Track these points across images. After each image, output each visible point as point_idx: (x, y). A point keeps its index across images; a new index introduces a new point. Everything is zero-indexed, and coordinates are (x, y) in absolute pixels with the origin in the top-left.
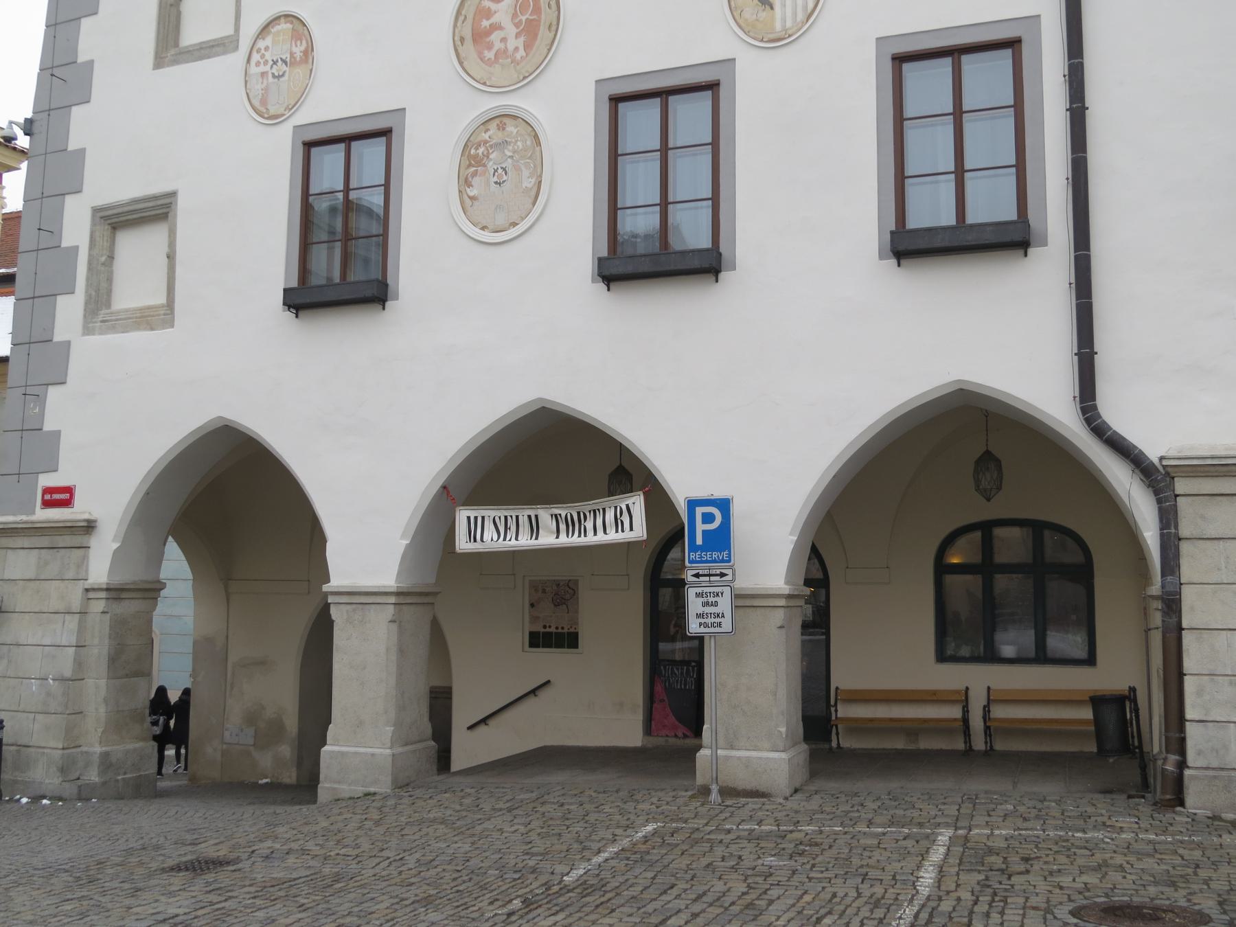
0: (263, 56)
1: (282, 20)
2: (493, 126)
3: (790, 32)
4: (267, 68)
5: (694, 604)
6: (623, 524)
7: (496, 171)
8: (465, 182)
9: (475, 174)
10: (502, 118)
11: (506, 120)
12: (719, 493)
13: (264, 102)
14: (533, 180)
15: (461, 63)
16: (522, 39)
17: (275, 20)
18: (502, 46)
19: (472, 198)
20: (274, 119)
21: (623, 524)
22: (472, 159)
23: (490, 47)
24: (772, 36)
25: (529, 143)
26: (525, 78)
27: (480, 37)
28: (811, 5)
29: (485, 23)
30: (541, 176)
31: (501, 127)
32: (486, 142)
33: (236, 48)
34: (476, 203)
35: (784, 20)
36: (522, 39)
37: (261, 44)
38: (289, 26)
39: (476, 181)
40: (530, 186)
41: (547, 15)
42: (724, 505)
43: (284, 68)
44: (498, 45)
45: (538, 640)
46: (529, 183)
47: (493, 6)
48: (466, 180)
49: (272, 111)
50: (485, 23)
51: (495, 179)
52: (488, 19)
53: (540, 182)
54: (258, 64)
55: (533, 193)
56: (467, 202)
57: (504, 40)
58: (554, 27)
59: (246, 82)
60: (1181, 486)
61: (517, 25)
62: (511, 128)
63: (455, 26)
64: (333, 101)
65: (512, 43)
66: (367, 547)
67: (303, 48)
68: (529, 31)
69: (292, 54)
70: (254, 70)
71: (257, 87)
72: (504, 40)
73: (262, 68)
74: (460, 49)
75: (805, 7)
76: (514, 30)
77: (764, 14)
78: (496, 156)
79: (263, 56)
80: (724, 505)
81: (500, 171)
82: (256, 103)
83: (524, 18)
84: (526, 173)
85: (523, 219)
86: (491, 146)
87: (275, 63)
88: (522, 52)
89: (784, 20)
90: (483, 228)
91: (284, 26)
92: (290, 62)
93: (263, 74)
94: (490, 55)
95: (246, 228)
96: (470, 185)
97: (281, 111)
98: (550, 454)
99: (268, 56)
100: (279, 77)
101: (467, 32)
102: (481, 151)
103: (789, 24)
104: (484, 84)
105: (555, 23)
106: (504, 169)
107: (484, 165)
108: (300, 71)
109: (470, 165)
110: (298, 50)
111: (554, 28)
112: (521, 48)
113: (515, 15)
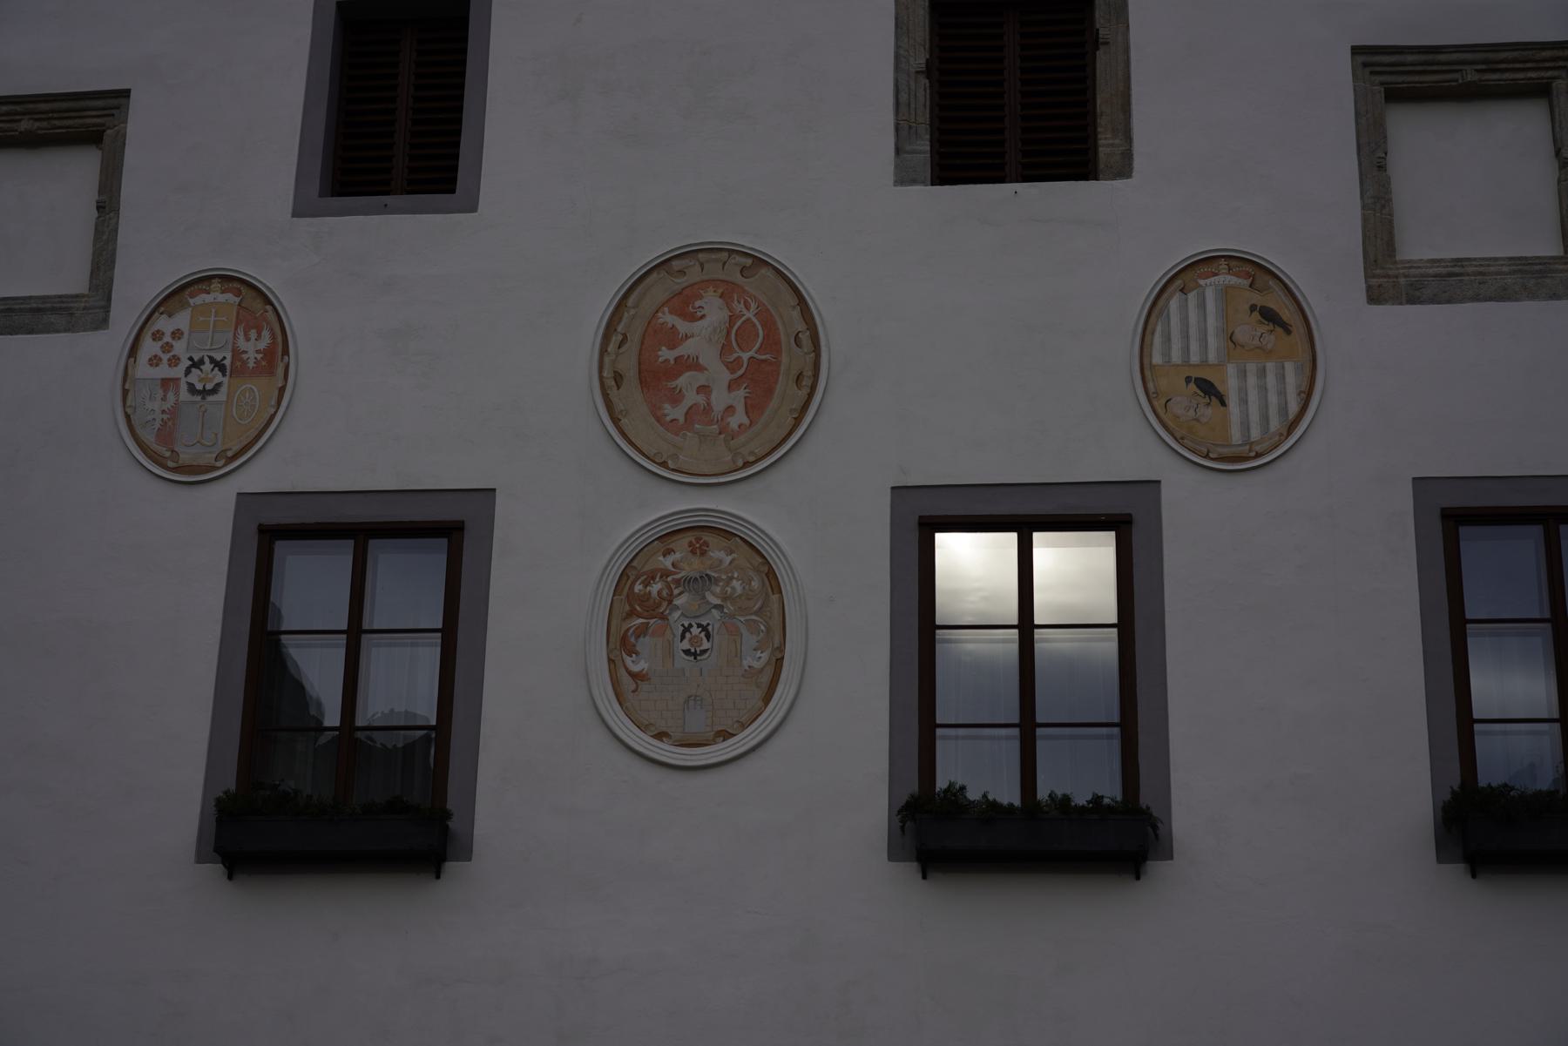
0: (167, 348)
1: (216, 285)
2: (682, 544)
3: (1258, 448)
4: (179, 372)
7: (687, 630)
8: (622, 644)
9: (642, 631)
11: (706, 537)
14: (765, 656)
15: (616, 421)
16: (741, 393)
18: (701, 399)
19: (635, 676)
20: (194, 474)
22: (637, 602)
23: (676, 398)
24: (1226, 451)
25: (755, 584)
26: (747, 464)
27: (655, 378)
28: (1293, 408)
29: (666, 354)
30: (781, 648)
31: (699, 550)
32: (665, 574)
33: (102, 323)
34: (644, 686)
35: (1246, 426)
36: (741, 393)
37: (164, 324)
38: (230, 297)
39: (644, 644)
40: (757, 665)
43: (218, 377)
44: (691, 398)
46: (757, 660)
47: (682, 326)
48: (624, 639)
49: (186, 457)
50: (666, 354)
51: (686, 645)
52: (672, 347)
53: (780, 661)
54: (154, 361)
55: (765, 679)
56: (627, 686)
57: (704, 389)
58: (809, 379)
59: (125, 393)
61: (732, 366)
62: (717, 554)
63: (603, 351)
65: (720, 399)
67: (264, 343)
68: (757, 382)
69: (237, 353)
70: (142, 369)
71: (152, 407)
72: (704, 389)
73: (164, 371)
74: (614, 393)
75: (1283, 410)
76: (726, 376)
77: (1209, 412)
79: (167, 348)
81: (695, 630)
82: (149, 438)
83: (745, 356)
84: (750, 640)
85: (744, 726)
86: (677, 582)
87: (196, 364)
88: (739, 418)
89: (1246, 426)
90: (660, 736)
91: (217, 296)
92: (236, 368)
93: (166, 383)
94: (676, 413)
96: (631, 651)
97: (209, 458)
99: (179, 348)
100: (204, 393)
101: (628, 364)
102: (655, 588)
103: (1255, 434)
104: (664, 464)
105: (808, 373)
106: (704, 628)
107: (663, 617)
109: (632, 614)
110: (252, 348)
111: (807, 382)
112: (740, 409)
113: (725, 349)
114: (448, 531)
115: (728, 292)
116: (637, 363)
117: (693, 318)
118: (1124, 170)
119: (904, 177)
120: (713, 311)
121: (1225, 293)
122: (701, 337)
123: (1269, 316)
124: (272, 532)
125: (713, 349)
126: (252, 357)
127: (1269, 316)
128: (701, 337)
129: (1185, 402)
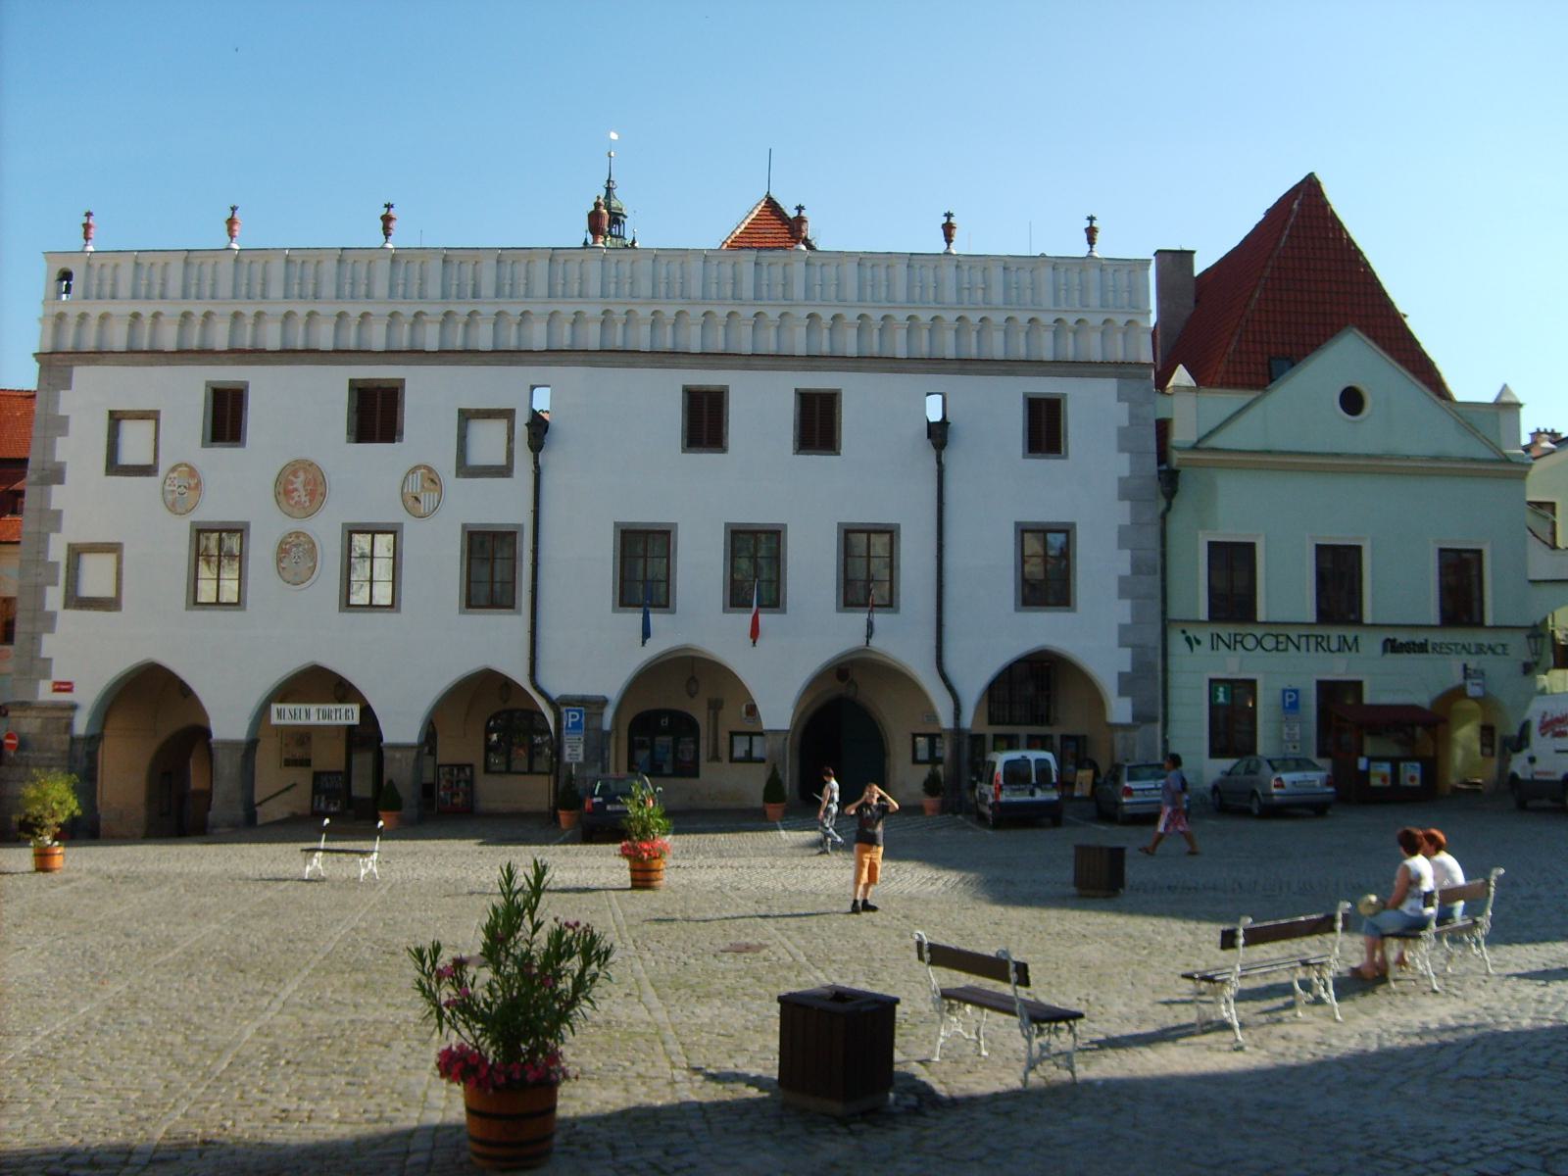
8: (279, 560)
10: (298, 534)
13: (173, 505)
17: (180, 465)
21: (348, 715)
22: (283, 551)
27: (288, 493)
29: (291, 487)
31: (298, 537)
39: (286, 560)
41: (320, 489)
44: (297, 499)
45: (289, 763)
46: (311, 564)
49: (179, 510)
56: (281, 571)
58: (324, 495)
60: (563, 709)
64: (213, 510)
65: (303, 499)
66: (228, 724)
68: (312, 494)
71: (170, 497)
73: (171, 488)
77: (417, 505)
88: (308, 504)
93: (173, 491)
94: (292, 502)
98: (317, 683)
101: (282, 491)
110: (193, 482)
114: (240, 530)
115: (306, 471)
116: (283, 490)
117: (297, 477)
118: (401, 440)
119: (348, 441)
120: (302, 476)
121: (422, 474)
122: (299, 482)
123: (432, 481)
124: (200, 531)
125: (302, 485)
126: (193, 485)
127: (432, 481)
128: (299, 482)
129: (411, 502)
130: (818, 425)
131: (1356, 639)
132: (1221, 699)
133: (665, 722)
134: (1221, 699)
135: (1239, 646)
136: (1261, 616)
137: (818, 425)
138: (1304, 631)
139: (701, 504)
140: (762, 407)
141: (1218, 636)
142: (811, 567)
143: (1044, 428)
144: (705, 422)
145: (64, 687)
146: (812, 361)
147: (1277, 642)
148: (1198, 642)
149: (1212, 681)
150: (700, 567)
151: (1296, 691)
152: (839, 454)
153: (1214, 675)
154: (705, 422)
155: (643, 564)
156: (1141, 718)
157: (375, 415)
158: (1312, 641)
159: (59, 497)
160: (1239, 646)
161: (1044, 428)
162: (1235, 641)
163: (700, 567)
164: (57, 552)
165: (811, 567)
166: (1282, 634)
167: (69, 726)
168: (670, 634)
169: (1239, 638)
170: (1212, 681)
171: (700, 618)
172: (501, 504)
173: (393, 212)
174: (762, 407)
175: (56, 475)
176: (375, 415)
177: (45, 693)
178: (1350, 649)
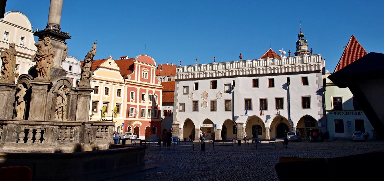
5: (215, 130)
6: (211, 125)
8: (203, 105)
12: (216, 124)
21: (211, 125)
42: (216, 125)
45: (208, 132)
46: (206, 105)
64: (195, 99)
68: (206, 96)
78: (205, 103)
80: (216, 125)
95: (189, 105)
98: (207, 121)
108: (192, 97)
122: (205, 95)
125: (205, 95)
128: (205, 95)
130: (271, 83)
131: (362, 112)
132: (337, 123)
133: (257, 126)
134: (337, 123)
135: (339, 114)
136: (343, 109)
137: (271, 83)
138: (352, 111)
139: (255, 96)
140: (263, 81)
141: (336, 113)
142: (271, 104)
143: (305, 81)
144: (256, 84)
145: (178, 122)
146: (271, 74)
147: (347, 113)
148: (332, 114)
149: (335, 120)
150: (256, 104)
151: (350, 121)
152: (274, 87)
153: (335, 119)
154: (256, 84)
155: (248, 104)
156: (323, 126)
157: (214, 85)
158: (353, 113)
159: (177, 98)
160: (339, 114)
161: (305, 81)
162: (339, 113)
163: (256, 104)
164: (178, 104)
165: (271, 104)
166: (347, 111)
167: (179, 127)
168: (251, 113)
169: (339, 113)
170: (335, 120)
171: (256, 111)
172: (229, 97)
173: (215, 58)
174: (263, 81)
175: (177, 95)
176: (214, 85)
177: (176, 123)
178: (361, 114)
